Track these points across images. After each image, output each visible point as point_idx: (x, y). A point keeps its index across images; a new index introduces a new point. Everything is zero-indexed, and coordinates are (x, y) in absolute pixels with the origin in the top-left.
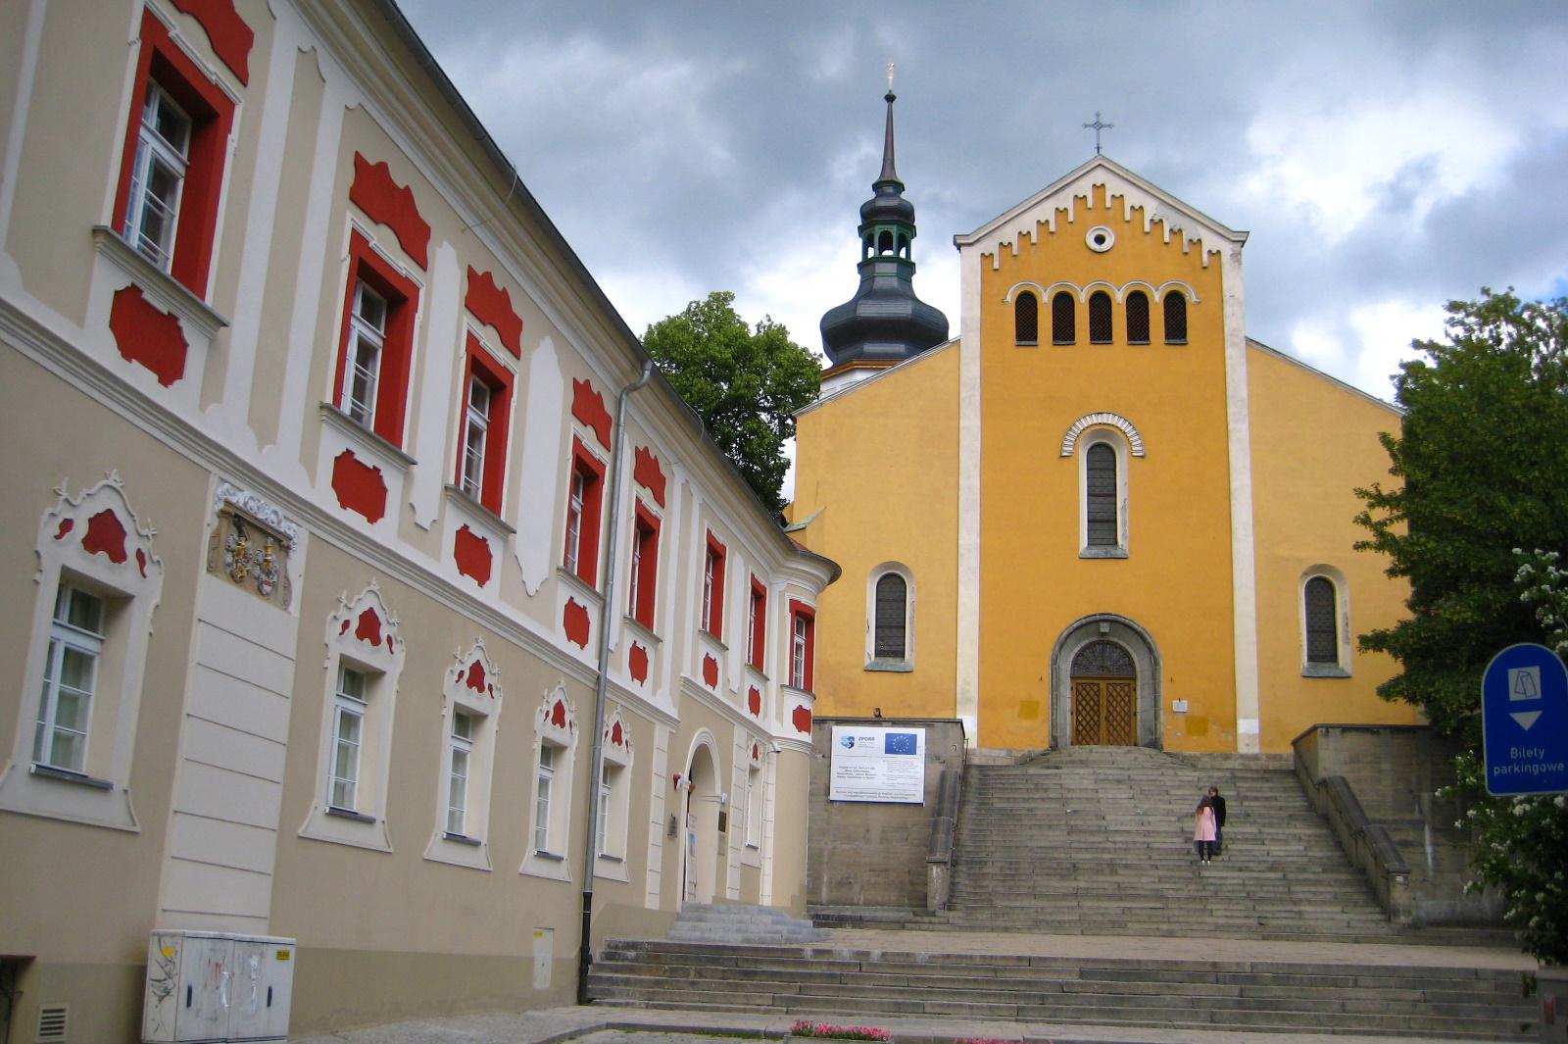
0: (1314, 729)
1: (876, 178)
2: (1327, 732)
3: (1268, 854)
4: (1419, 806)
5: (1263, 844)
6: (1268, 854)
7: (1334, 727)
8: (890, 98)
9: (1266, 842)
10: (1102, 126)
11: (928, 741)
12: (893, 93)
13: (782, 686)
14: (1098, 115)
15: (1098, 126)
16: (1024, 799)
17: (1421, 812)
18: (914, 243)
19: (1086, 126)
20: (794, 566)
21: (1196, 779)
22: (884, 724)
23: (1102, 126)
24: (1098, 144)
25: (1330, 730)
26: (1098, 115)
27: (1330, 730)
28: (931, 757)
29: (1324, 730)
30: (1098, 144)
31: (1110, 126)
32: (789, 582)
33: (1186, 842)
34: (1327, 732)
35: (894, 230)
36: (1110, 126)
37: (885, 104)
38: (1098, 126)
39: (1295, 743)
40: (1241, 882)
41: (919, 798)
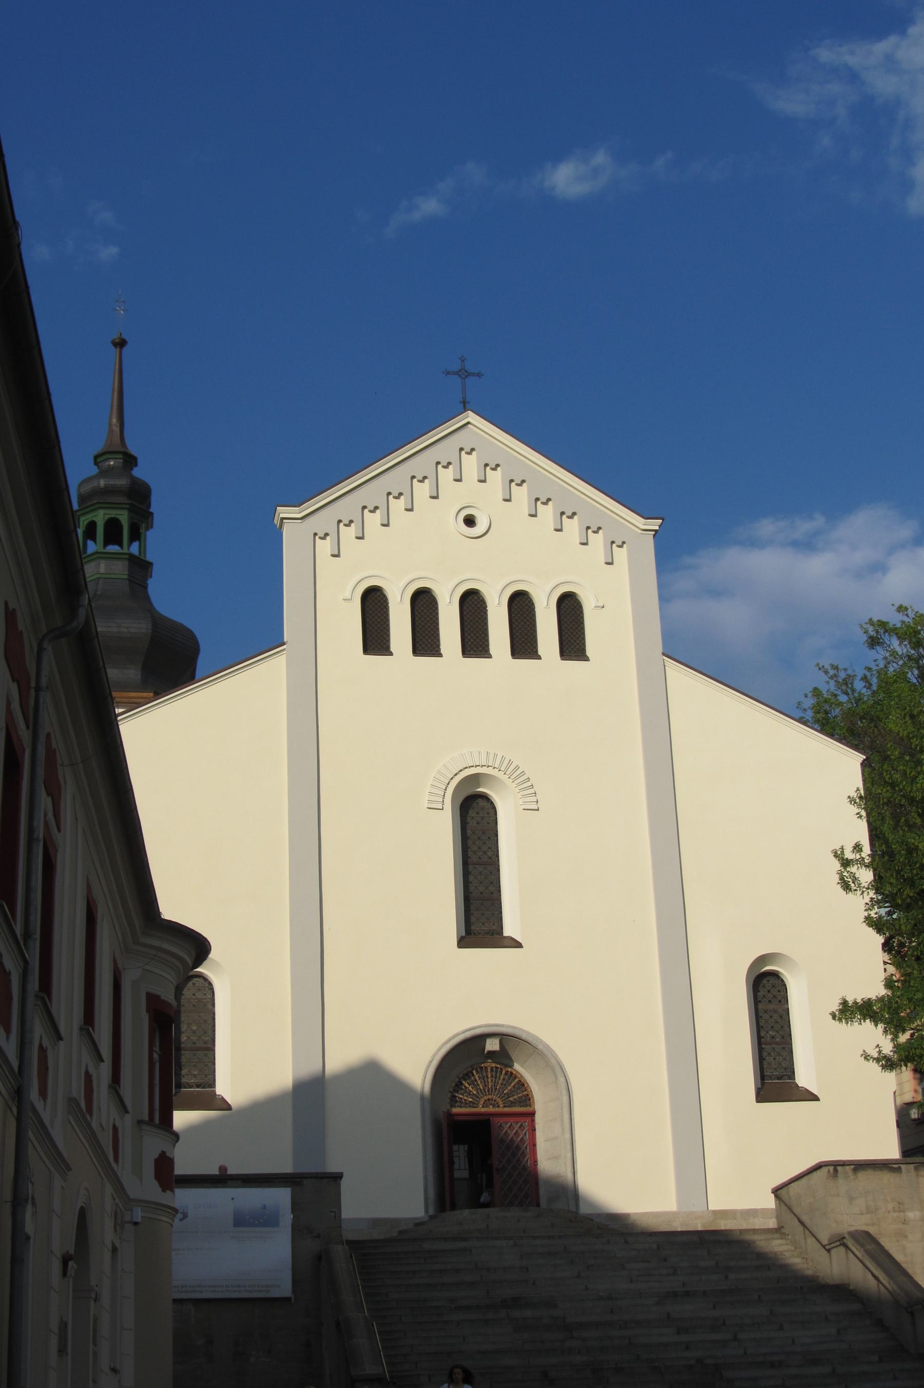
0: (818, 1167)
1: (99, 448)
2: (836, 1171)
3: (793, 1341)
5: (781, 1328)
6: (793, 1341)
7: (844, 1164)
8: (121, 344)
10: (469, 375)
11: (296, 1206)
12: (124, 336)
13: (140, 1122)
14: (463, 360)
15: (464, 374)
18: (152, 536)
19: (448, 373)
20: (156, 943)
21: (655, 1246)
24: (464, 398)
25: (839, 1168)
26: (463, 360)
27: (839, 1168)
28: (299, 1231)
29: (831, 1168)
30: (464, 398)
31: (479, 375)
32: (147, 967)
33: (678, 1333)
34: (836, 1171)
35: (124, 517)
36: (479, 375)
37: (114, 351)
38: (464, 374)
39: (776, 1191)
41: (285, 1289)
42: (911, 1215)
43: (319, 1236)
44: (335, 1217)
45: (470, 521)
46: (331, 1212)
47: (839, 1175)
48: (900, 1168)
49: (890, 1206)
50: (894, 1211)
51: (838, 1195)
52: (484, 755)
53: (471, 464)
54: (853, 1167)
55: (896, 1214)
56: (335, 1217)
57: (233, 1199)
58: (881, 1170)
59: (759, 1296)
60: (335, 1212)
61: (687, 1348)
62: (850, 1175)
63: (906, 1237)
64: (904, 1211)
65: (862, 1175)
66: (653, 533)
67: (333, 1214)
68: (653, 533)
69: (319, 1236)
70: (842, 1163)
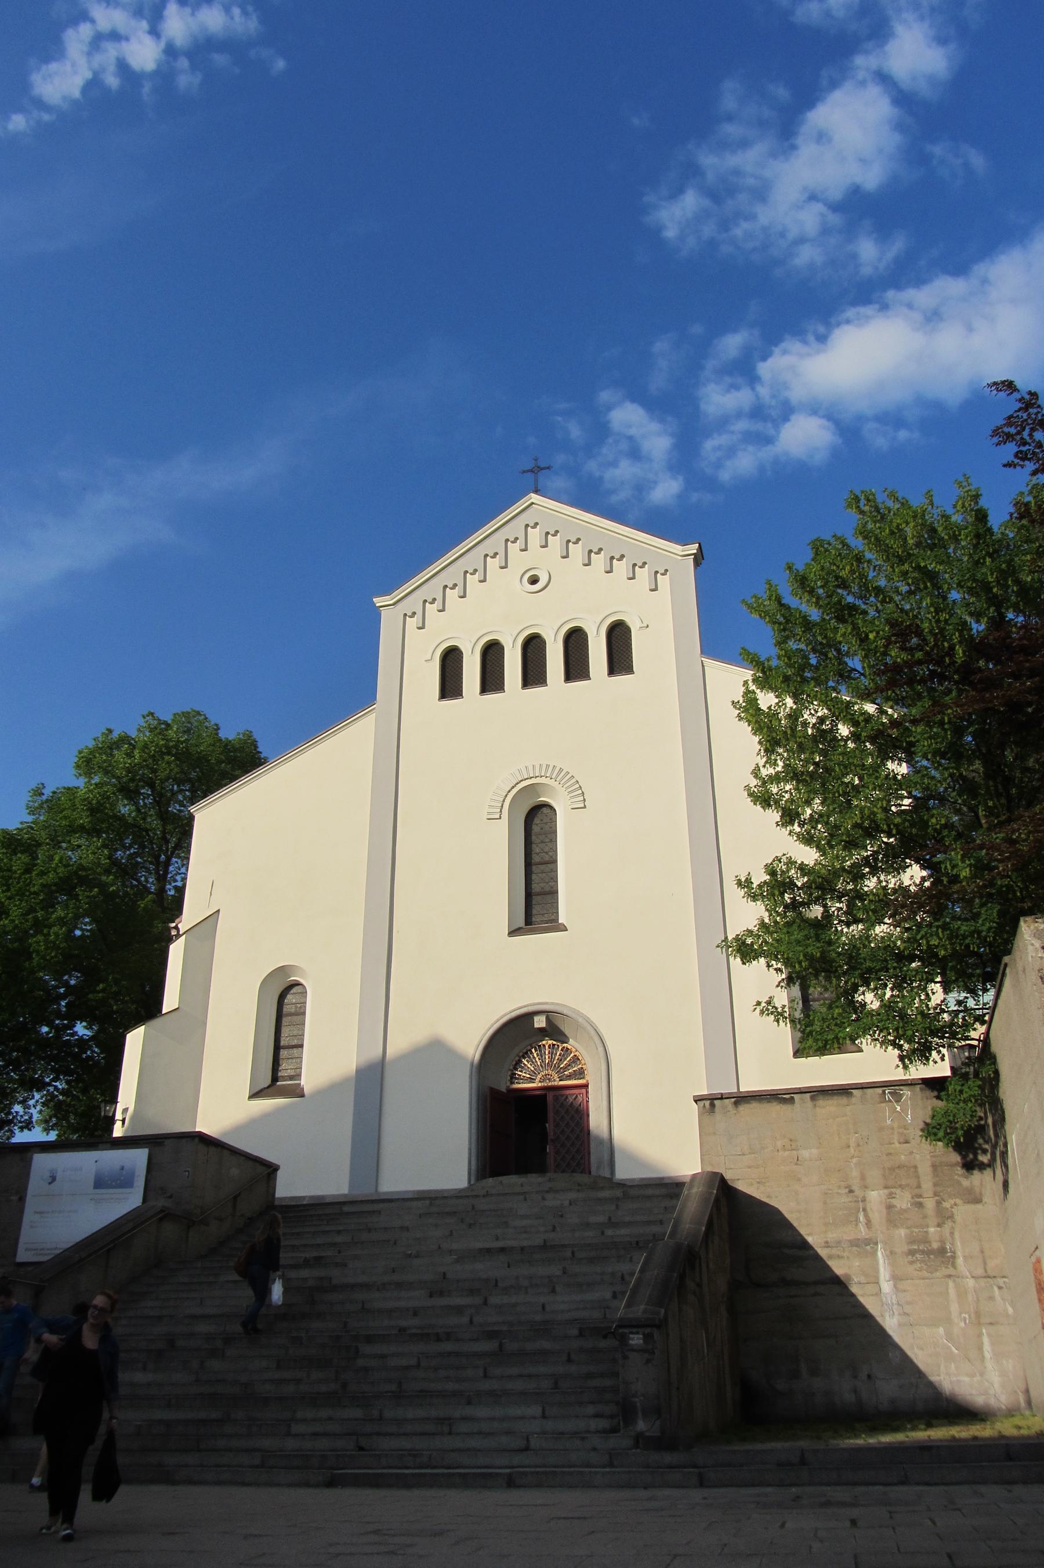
2: (712, 1105)
4: (866, 1216)
9: (558, 1289)
16: (293, 1246)
17: (869, 1223)
22: (100, 1146)
23: (532, 471)
25: (716, 1102)
29: (707, 1103)
33: (431, 1296)
34: (712, 1105)
40: (413, 1362)
42: (805, 1154)
43: (171, 1197)
44: (188, 1177)
45: (534, 581)
46: (185, 1171)
47: (717, 1109)
48: (792, 1098)
49: (779, 1144)
50: (785, 1150)
51: (715, 1134)
52: (531, 768)
53: (535, 535)
54: (733, 1100)
55: (787, 1153)
56: (188, 1177)
57: (96, 1162)
58: (768, 1102)
59: (573, 1253)
60: (188, 1171)
61: (415, 1314)
62: (731, 1109)
63: (799, 1180)
64: (796, 1149)
65: (744, 1108)
66: (693, 557)
67: (187, 1173)
68: (693, 557)
69: (171, 1197)
70: (720, 1097)
